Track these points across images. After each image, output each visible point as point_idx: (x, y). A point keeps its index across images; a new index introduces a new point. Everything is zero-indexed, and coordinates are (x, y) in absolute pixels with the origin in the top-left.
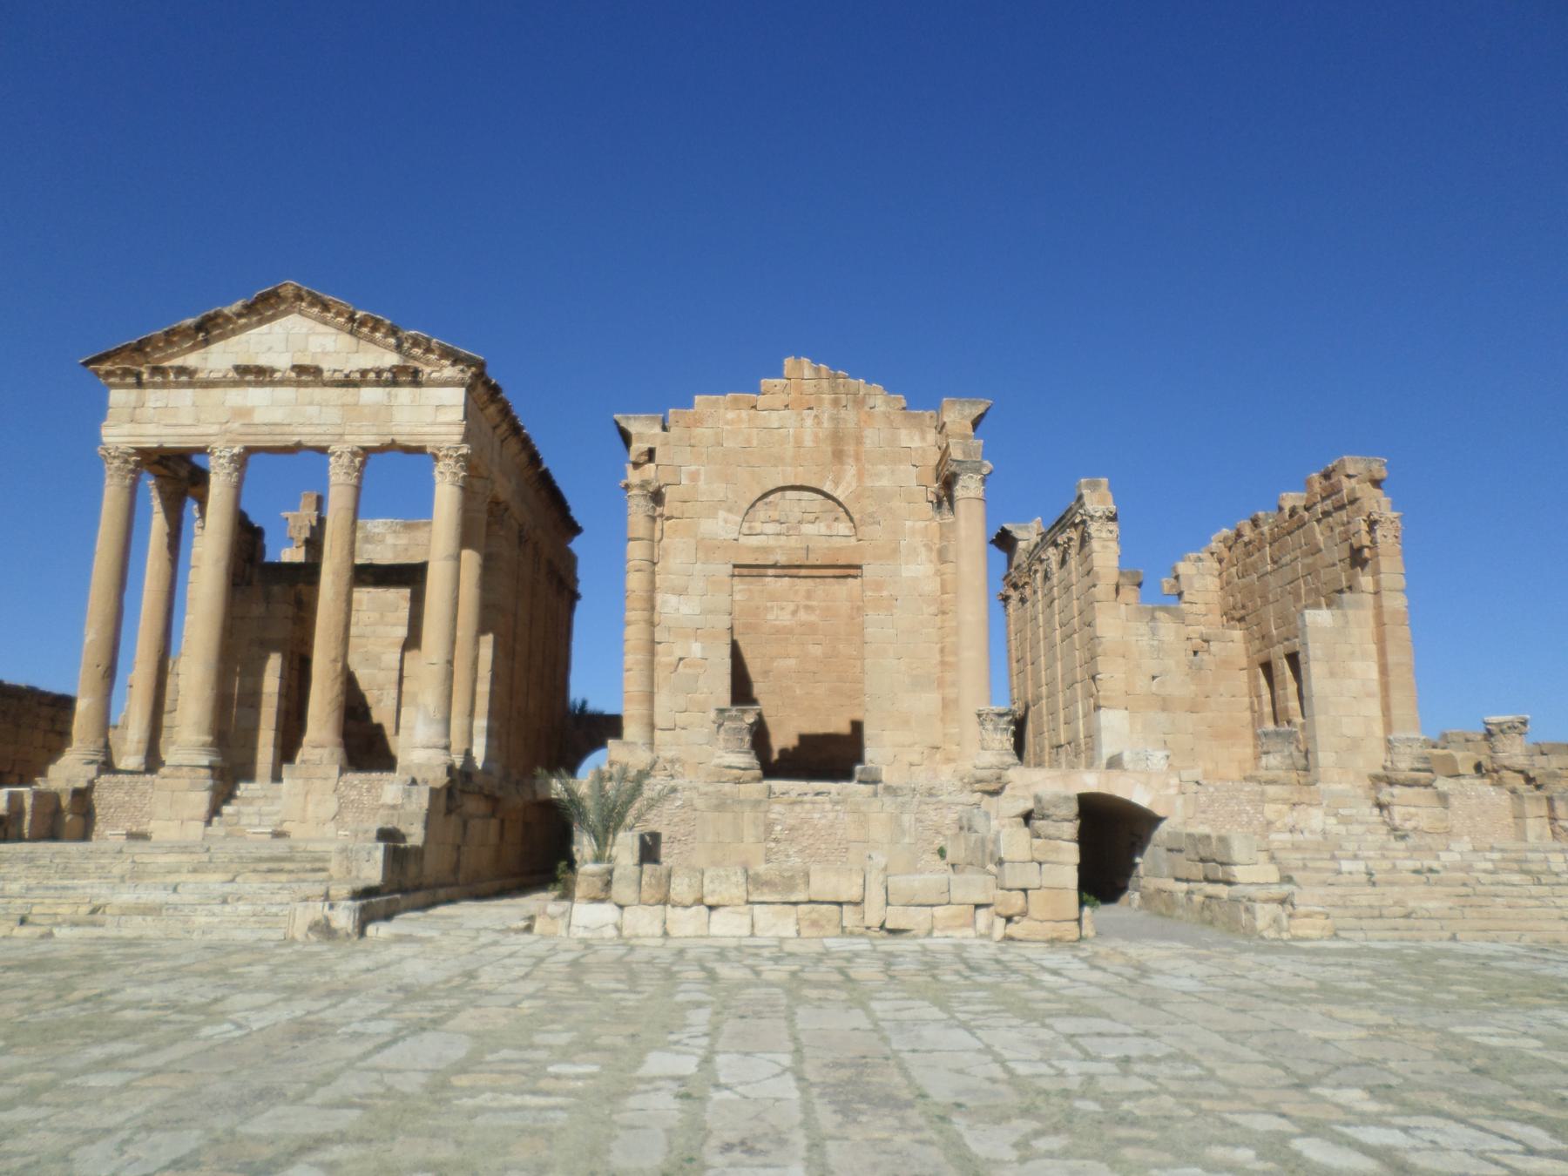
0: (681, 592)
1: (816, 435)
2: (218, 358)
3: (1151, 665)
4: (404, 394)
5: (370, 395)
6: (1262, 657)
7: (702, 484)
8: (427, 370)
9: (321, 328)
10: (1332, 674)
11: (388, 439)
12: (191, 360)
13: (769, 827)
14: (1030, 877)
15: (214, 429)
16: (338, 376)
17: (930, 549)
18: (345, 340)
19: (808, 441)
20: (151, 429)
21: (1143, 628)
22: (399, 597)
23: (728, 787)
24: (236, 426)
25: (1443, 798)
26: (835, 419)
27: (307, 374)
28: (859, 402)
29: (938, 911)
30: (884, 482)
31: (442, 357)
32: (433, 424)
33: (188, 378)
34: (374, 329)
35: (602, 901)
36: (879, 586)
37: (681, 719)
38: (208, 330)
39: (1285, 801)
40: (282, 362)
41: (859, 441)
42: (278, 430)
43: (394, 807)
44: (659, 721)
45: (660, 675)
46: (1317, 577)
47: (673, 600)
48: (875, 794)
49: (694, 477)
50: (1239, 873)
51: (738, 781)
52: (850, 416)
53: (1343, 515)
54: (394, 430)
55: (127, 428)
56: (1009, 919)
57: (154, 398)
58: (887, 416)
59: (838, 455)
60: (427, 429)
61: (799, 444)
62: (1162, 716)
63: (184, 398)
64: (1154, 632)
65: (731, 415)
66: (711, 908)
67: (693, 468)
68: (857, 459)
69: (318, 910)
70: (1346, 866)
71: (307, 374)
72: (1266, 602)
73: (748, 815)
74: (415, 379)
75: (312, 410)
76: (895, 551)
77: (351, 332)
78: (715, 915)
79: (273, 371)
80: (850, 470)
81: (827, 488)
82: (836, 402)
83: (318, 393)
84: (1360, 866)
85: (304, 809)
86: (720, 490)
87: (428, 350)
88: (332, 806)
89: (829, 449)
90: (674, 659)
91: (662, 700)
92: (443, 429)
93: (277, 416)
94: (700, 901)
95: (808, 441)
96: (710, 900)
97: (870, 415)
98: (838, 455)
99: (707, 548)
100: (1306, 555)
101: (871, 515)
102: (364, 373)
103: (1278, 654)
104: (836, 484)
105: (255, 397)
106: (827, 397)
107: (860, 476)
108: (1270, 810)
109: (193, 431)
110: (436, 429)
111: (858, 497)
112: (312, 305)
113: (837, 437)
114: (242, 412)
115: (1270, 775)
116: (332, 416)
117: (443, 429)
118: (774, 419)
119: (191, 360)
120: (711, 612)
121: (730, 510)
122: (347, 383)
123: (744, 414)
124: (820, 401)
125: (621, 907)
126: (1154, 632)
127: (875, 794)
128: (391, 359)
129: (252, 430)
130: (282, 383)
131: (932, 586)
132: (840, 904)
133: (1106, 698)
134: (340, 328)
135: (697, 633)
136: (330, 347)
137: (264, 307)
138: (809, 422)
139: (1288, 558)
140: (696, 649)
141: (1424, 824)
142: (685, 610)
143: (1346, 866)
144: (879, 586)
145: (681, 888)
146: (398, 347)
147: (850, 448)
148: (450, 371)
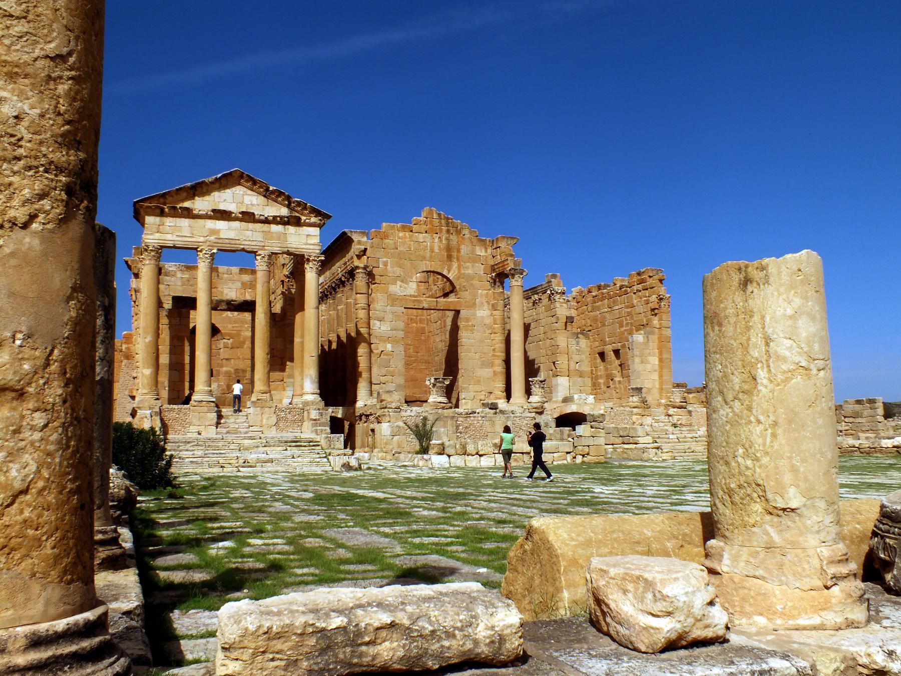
0: (381, 320)
1: (439, 247)
2: (200, 204)
3: (576, 358)
4: (291, 229)
5: (275, 228)
6: (599, 349)
7: (389, 267)
8: (303, 218)
9: (250, 192)
10: (642, 362)
11: (286, 250)
13: (457, 427)
14: (591, 442)
15: (202, 239)
16: (262, 218)
17: (489, 304)
18: (262, 199)
19: (436, 250)
20: (169, 237)
21: (574, 342)
22: (247, 316)
23: (440, 411)
24: (212, 238)
25: (690, 412)
26: (448, 239)
27: (248, 217)
28: (458, 232)
29: (555, 455)
31: (310, 212)
32: (307, 244)
33: (188, 213)
34: (278, 196)
35: (442, 454)
36: (467, 320)
37: (383, 379)
38: (198, 190)
39: (639, 414)
40: (232, 207)
41: (459, 251)
42: (233, 242)
43: (315, 420)
44: (374, 381)
45: (373, 359)
46: (632, 318)
47: (378, 323)
48: (496, 413)
49: (385, 264)
50: (641, 440)
51: (443, 408)
52: (454, 238)
53: (647, 293)
54: (289, 246)
55: (157, 235)
56: (583, 456)
57: (169, 222)
58: (470, 239)
59: (450, 257)
60: (304, 246)
61: (432, 251)
62: (580, 379)
63: (185, 223)
64: (578, 343)
65: (401, 234)
66: (481, 456)
67: (385, 259)
68: (458, 259)
69: (345, 459)
70: (671, 436)
71: (248, 217)
72: (604, 325)
73: (449, 422)
74: (297, 223)
75: (249, 233)
76: (474, 304)
77: (264, 196)
78: (482, 458)
79: (231, 213)
80: (455, 265)
81: (445, 273)
82: (448, 231)
84: (675, 436)
85: (262, 421)
86: (398, 271)
87: (305, 208)
88: (274, 420)
90: (379, 351)
91: (375, 370)
92: (311, 247)
93: (232, 235)
94: (477, 454)
95: (436, 250)
96: (480, 453)
97: (463, 239)
98: (450, 257)
99: (393, 300)
100: (627, 307)
101: (464, 287)
102: (275, 217)
103: (608, 350)
104: (449, 271)
105: (221, 225)
107: (459, 268)
108: (634, 418)
109: (191, 239)
110: (308, 247)
111: (458, 278)
112: (247, 181)
113: (449, 249)
114: (213, 232)
115: (635, 404)
116: (259, 237)
117: (311, 247)
118: (421, 237)
120: (395, 330)
121: (402, 281)
122: (266, 221)
123: (407, 234)
124: (441, 230)
125: (449, 456)
126: (578, 343)
127: (496, 413)
128: (284, 211)
129: (221, 241)
130: (236, 219)
131: (488, 321)
132: (523, 453)
133: (560, 372)
134: (259, 193)
135: (388, 339)
136: (255, 202)
137: (226, 182)
138: (436, 240)
139: (617, 307)
140: (389, 347)
141: (684, 423)
142: (383, 328)
143: (671, 436)
144: (467, 320)
145: (470, 448)
146: (288, 206)
147: (455, 254)
148: (313, 220)
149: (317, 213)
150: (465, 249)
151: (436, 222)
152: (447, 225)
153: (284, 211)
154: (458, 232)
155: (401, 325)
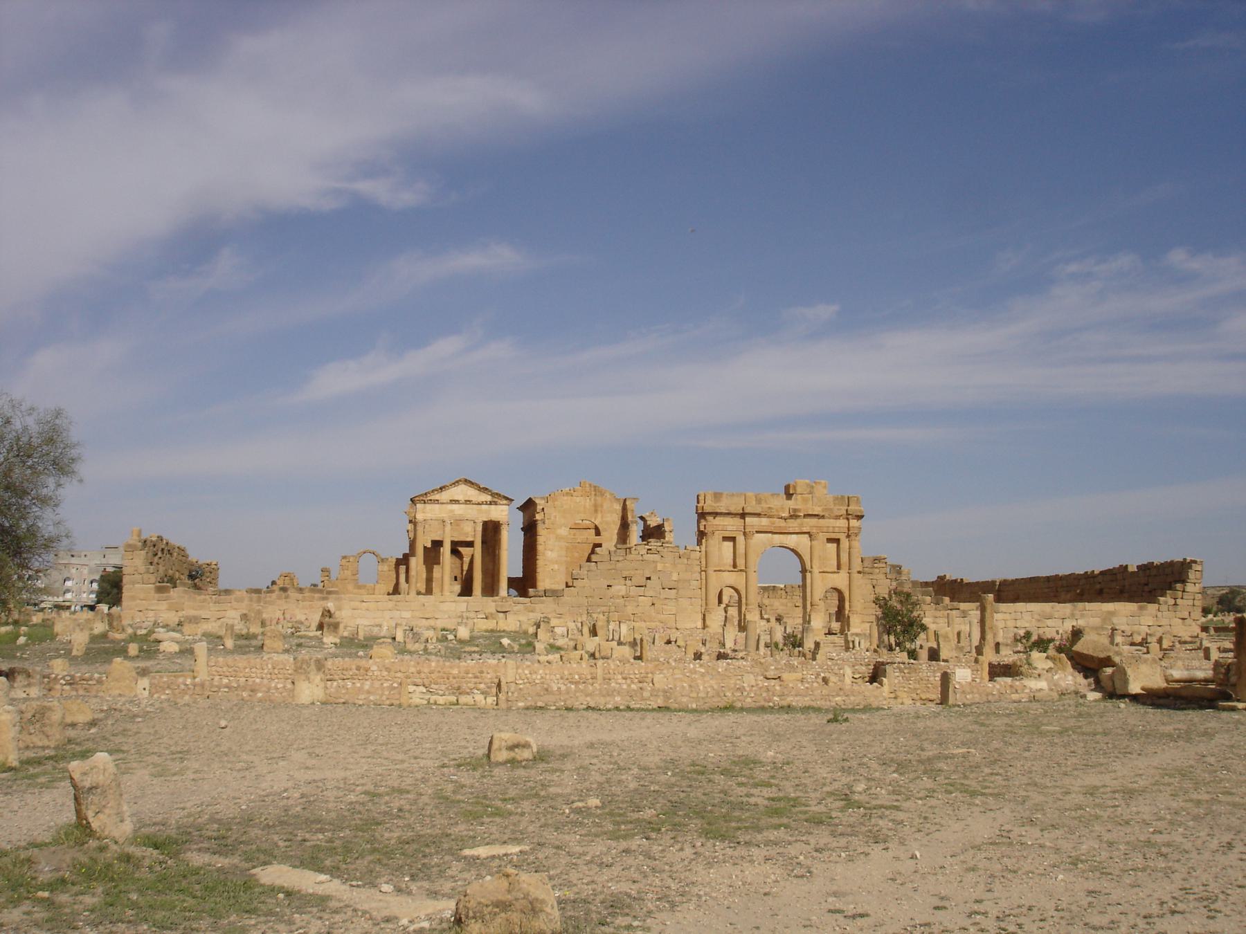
4: (493, 507)
5: (484, 507)
27: (468, 502)
28: (602, 495)
40: (461, 498)
52: (599, 499)
57: (428, 506)
59: (596, 511)
71: (468, 502)
80: (599, 515)
98: (596, 511)
99: (559, 538)
105: (455, 507)
114: (452, 511)
118: (578, 499)
119: (436, 496)
128: (489, 498)
135: (556, 562)
140: (556, 567)
149: (507, 498)
150: (606, 505)
153: (489, 498)
154: (602, 495)
155: (564, 553)
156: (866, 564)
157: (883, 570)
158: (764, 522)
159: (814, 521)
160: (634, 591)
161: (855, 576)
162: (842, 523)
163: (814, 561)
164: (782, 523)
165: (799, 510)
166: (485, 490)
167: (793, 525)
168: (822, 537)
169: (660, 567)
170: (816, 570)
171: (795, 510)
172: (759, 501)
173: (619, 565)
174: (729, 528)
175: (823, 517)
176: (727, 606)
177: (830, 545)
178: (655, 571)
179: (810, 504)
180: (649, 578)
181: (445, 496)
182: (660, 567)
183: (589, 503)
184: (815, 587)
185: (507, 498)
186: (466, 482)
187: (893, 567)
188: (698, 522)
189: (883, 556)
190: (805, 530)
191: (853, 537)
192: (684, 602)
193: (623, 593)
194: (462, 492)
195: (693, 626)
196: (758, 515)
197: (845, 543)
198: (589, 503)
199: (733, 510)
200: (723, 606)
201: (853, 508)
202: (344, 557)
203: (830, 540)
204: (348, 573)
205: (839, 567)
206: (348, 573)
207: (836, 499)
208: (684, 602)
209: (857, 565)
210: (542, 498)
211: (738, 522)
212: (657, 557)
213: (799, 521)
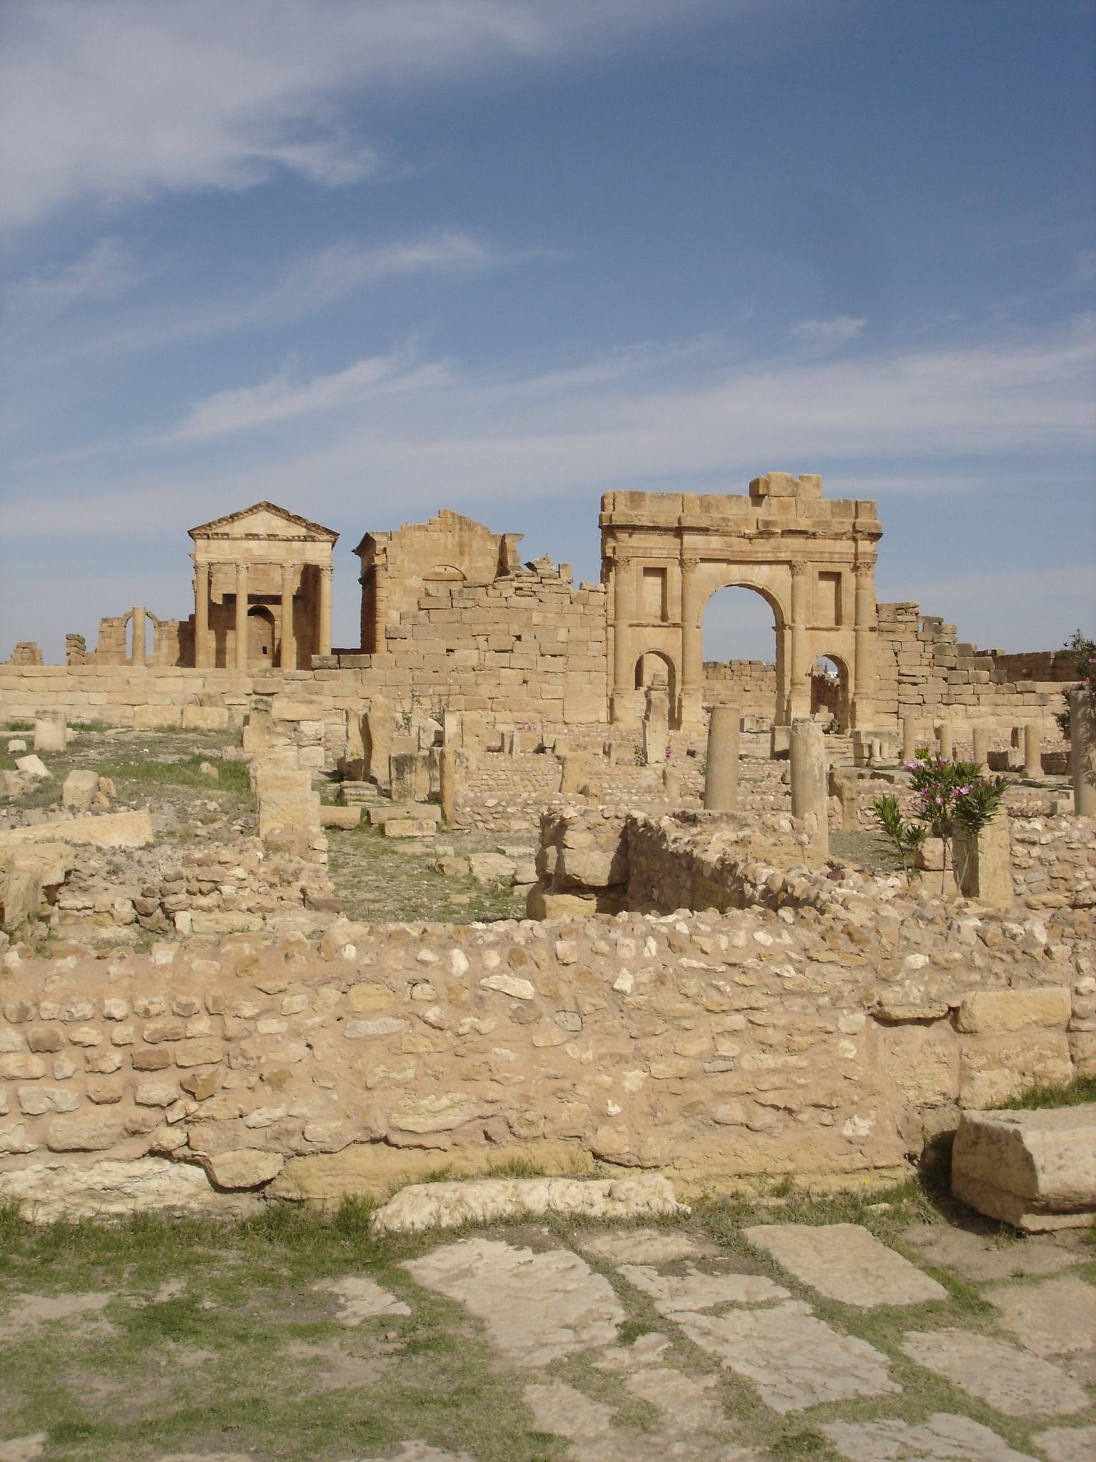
4: (309, 544)
5: (296, 545)
12: (226, 529)
19: (449, 546)
26: (461, 537)
27: (272, 537)
30: (480, 565)
33: (226, 536)
40: (261, 531)
41: (470, 546)
49: (403, 561)
59: (462, 553)
61: (446, 547)
65: (417, 534)
71: (272, 537)
74: (313, 540)
80: (467, 559)
82: (461, 529)
83: (276, 543)
89: (457, 549)
95: (449, 546)
98: (462, 553)
99: (408, 591)
105: (253, 544)
106: (458, 526)
107: (470, 562)
114: (247, 550)
119: (226, 529)
147: (467, 550)
148: (326, 537)
150: (476, 545)
151: (450, 521)
152: (460, 523)
153: (303, 532)
156: (883, 616)
157: (911, 627)
158: (715, 542)
159: (798, 542)
160: (492, 659)
161: (867, 635)
162: (845, 546)
163: (798, 610)
164: (745, 545)
165: (773, 523)
166: (297, 519)
167: (764, 548)
168: (812, 569)
169: (536, 618)
170: (800, 626)
171: (767, 523)
172: (706, 506)
173: (467, 614)
174: (656, 553)
175: (814, 536)
176: (650, 689)
177: (823, 584)
178: (529, 625)
179: (791, 515)
180: (519, 638)
181: (238, 528)
182: (536, 618)
183: (450, 540)
184: (799, 653)
185: (329, 532)
186: (270, 507)
187: (928, 620)
188: (604, 543)
189: (913, 602)
190: (783, 557)
191: (863, 570)
192: (578, 679)
193: (474, 662)
194: (263, 522)
195: (592, 718)
196: (705, 531)
197: (849, 580)
198: (450, 540)
199: (662, 522)
200: (643, 689)
201: (864, 520)
202: (105, 620)
203: (824, 575)
204: (112, 642)
205: (838, 620)
206: (112, 642)
207: (836, 505)
208: (578, 679)
209: (869, 618)
210: (385, 534)
211: (670, 541)
212: (532, 602)
213: (772, 541)
